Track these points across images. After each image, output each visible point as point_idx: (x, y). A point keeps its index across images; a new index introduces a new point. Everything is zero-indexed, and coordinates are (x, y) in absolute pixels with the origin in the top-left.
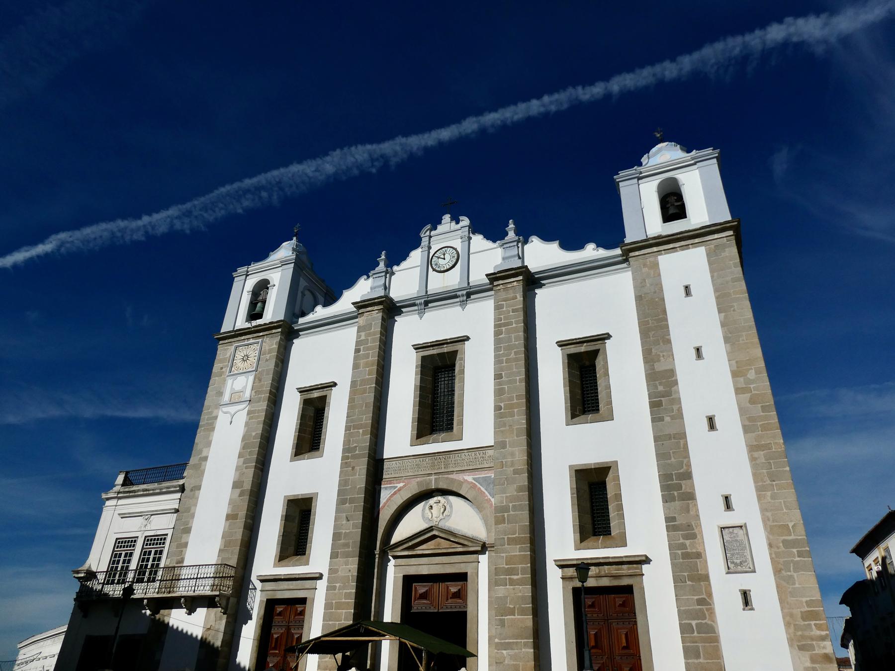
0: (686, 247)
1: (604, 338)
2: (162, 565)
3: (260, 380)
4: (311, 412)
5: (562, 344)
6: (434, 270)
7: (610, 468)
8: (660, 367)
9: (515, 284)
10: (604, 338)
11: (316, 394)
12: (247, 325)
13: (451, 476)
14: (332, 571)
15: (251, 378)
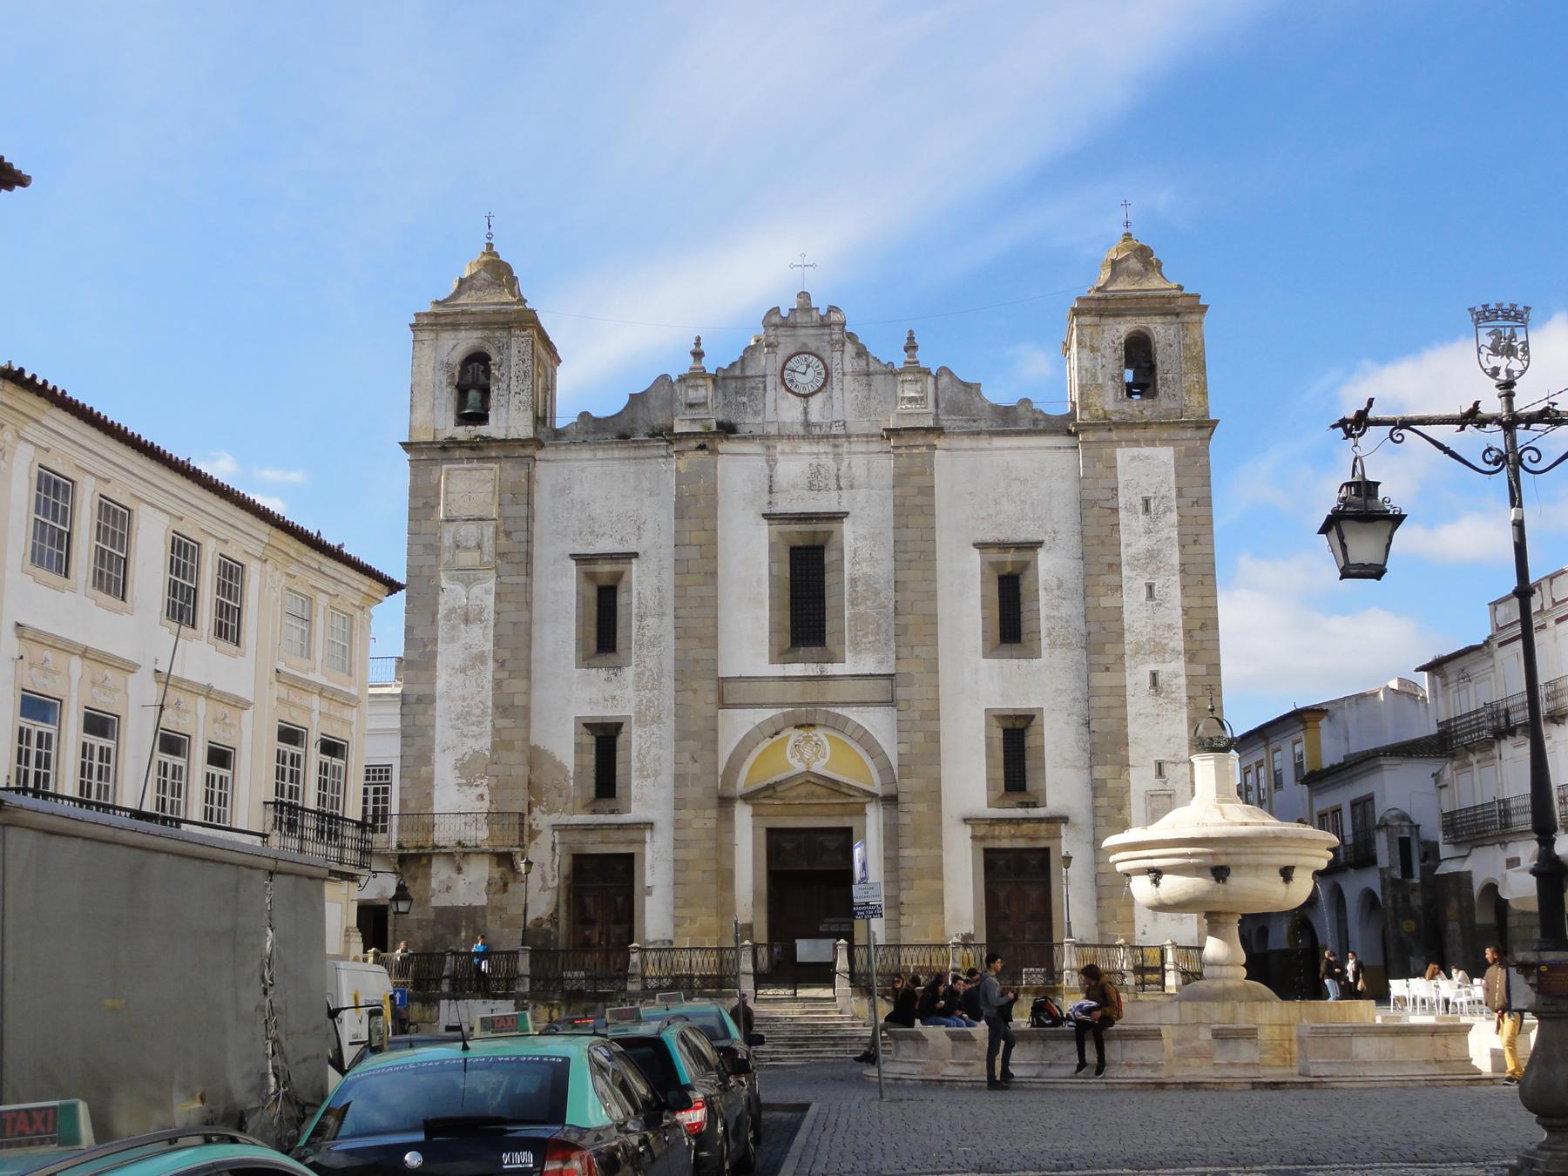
0: (1151, 443)
1: (1034, 546)
2: (394, 808)
3: (508, 534)
4: (592, 593)
5: (981, 546)
6: (788, 389)
7: (1032, 717)
8: (1106, 602)
9: (924, 449)
10: (1034, 546)
11: (605, 568)
12: (462, 433)
13: (832, 710)
14: (678, 825)
15: (489, 530)
